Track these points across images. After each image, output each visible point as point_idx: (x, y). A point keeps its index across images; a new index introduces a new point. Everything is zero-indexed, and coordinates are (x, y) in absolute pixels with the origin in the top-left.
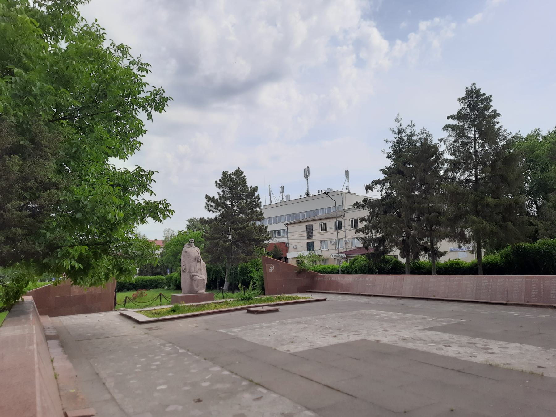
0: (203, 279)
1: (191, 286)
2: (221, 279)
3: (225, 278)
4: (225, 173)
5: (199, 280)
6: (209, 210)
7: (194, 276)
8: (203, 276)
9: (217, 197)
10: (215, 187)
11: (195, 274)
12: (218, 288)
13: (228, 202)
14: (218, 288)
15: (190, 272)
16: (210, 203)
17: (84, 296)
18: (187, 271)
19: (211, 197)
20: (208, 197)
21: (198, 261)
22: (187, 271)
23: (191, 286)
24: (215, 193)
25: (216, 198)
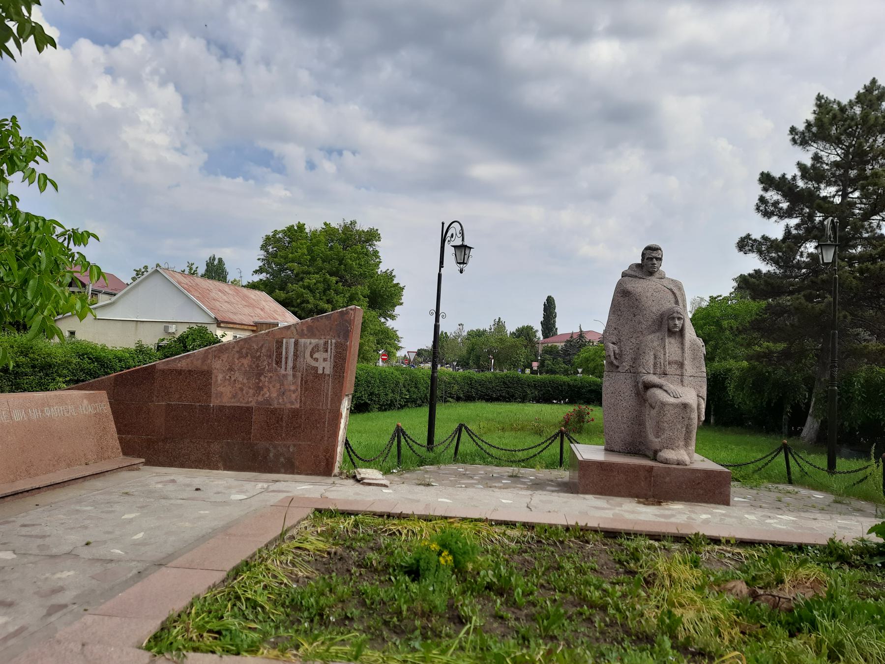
0: (685, 406)
1: (639, 422)
2: (796, 408)
3: (808, 406)
4: (822, 104)
5: (663, 404)
6: (767, 214)
7: (648, 386)
8: (691, 393)
9: (791, 171)
10: (790, 143)
11: (655, 379)
12: (785, 429)
13: (827, 191)
14: (785, 429)
15: (634, 372)
16: (773, 196)
17: (249, 410)
18: (626, 365)
19: (777, 174)
20: (767, 180)
21: (671, 333)
22: (626, 365)
23: (639, 422)
24: (788, 161)
25: (789, 177)
